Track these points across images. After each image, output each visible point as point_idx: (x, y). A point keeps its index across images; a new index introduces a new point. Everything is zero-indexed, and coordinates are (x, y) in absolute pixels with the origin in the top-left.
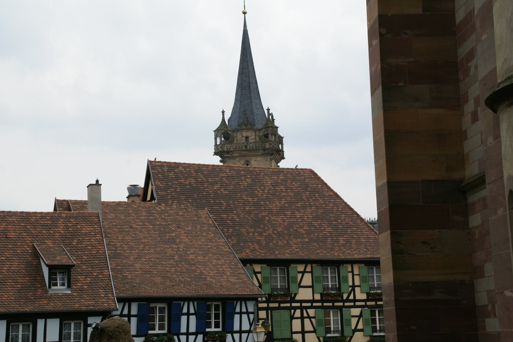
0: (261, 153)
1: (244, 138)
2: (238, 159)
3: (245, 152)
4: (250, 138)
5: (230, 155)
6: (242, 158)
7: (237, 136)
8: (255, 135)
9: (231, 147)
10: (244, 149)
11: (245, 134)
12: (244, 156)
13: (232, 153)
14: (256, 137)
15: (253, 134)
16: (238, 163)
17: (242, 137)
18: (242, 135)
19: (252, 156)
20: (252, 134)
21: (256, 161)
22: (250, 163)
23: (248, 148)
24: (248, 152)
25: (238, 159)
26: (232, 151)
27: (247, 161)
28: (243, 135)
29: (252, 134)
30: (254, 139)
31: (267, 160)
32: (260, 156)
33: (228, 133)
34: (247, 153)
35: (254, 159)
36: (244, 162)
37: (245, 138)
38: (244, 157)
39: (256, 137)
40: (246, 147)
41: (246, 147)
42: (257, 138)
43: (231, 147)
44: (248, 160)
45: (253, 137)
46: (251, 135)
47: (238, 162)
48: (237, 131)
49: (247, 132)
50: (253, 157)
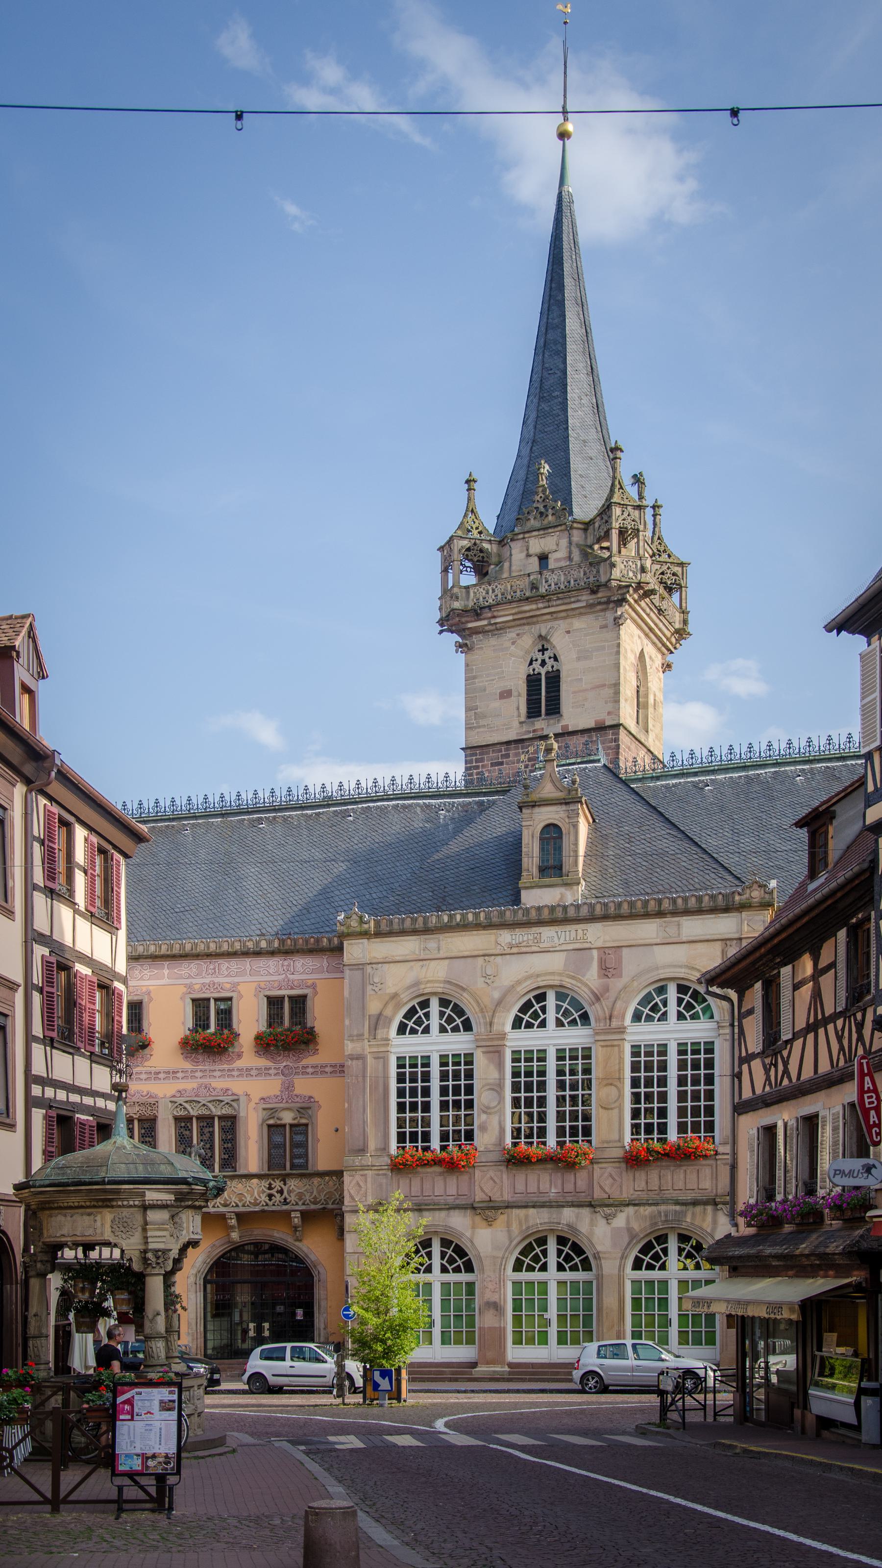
0: (583, 604)
1: (535, 561)
2: (511, 634)
3: (534, 607)
4: (552, 557)
5: (485, 622)
6: (526, 627)
7: (511, 555)
8: (570, 543)
9: (487, 593)
10: (528, 594)
11: (537, 545)
12: (530, 620)
13: (489, 615)
14: (570, 553)
15: (564, 542)
16: (513, 648)
17: (529, 555)
18: (527, 550)
19: (556, 619)
20: (557, 545)
21: (568, 632)
22: (548, 641)
23: (542, 590)
24: (541, 605)
25: (513, 635)
26: (490, 607)
27: (540, 636)
28: (531, 551)
29: (557, 545)
30: (565, 558)
31: (604, 627)
32: (581, 614)
33: (481, 551)
34: (538, 609)
35: (562, 625)
36: (530, 642)
37: (536, 559)
38: (534, 623)
39: (570, 553)
40: (534, 587)
41: (534, 587)
42: (576, 556)
43: (487, 593)
44: (543, 634)
45: (562, 553)
46: (555, 547)
47: (513, 643)
48: (512, 540)
49: (543, 537)
50: (561, 622)
